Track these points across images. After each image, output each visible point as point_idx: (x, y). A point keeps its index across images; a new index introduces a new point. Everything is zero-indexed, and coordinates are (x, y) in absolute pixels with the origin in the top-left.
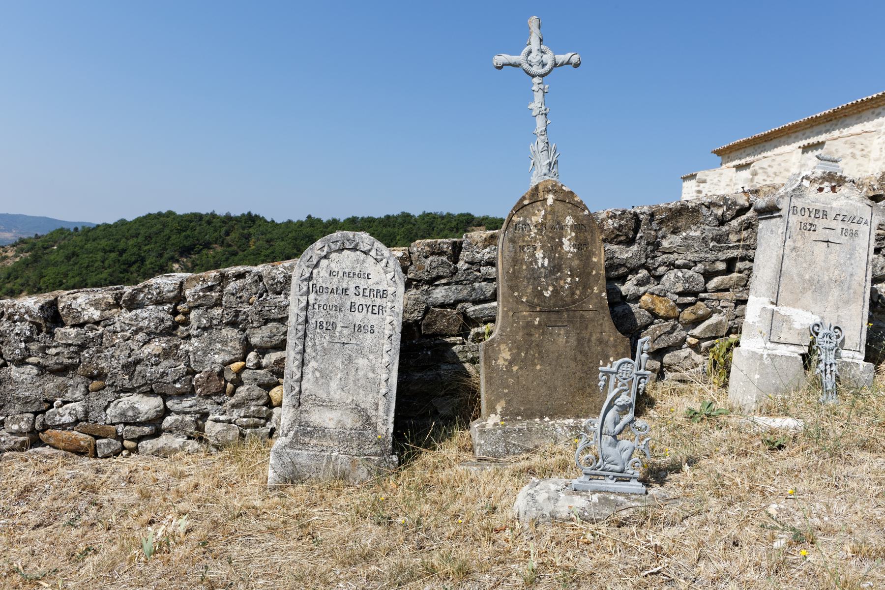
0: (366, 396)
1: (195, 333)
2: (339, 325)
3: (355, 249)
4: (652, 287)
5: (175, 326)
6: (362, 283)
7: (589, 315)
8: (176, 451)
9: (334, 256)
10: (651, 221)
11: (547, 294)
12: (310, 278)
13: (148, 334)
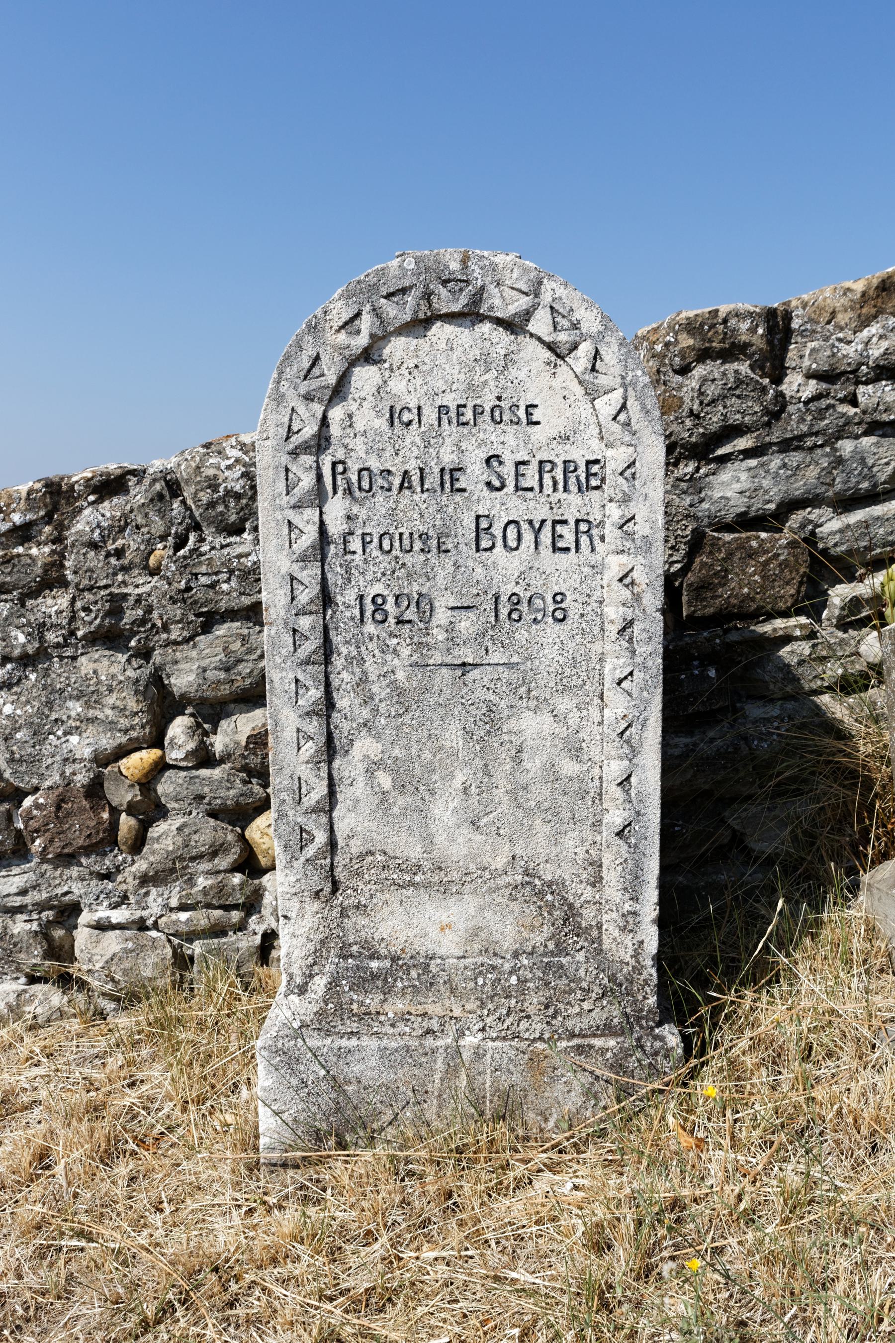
0: (555, 839)
2: (443, 602)
3: (471, 315)
6: (510, 444)
9: (397, 348)
12: (321, 441)
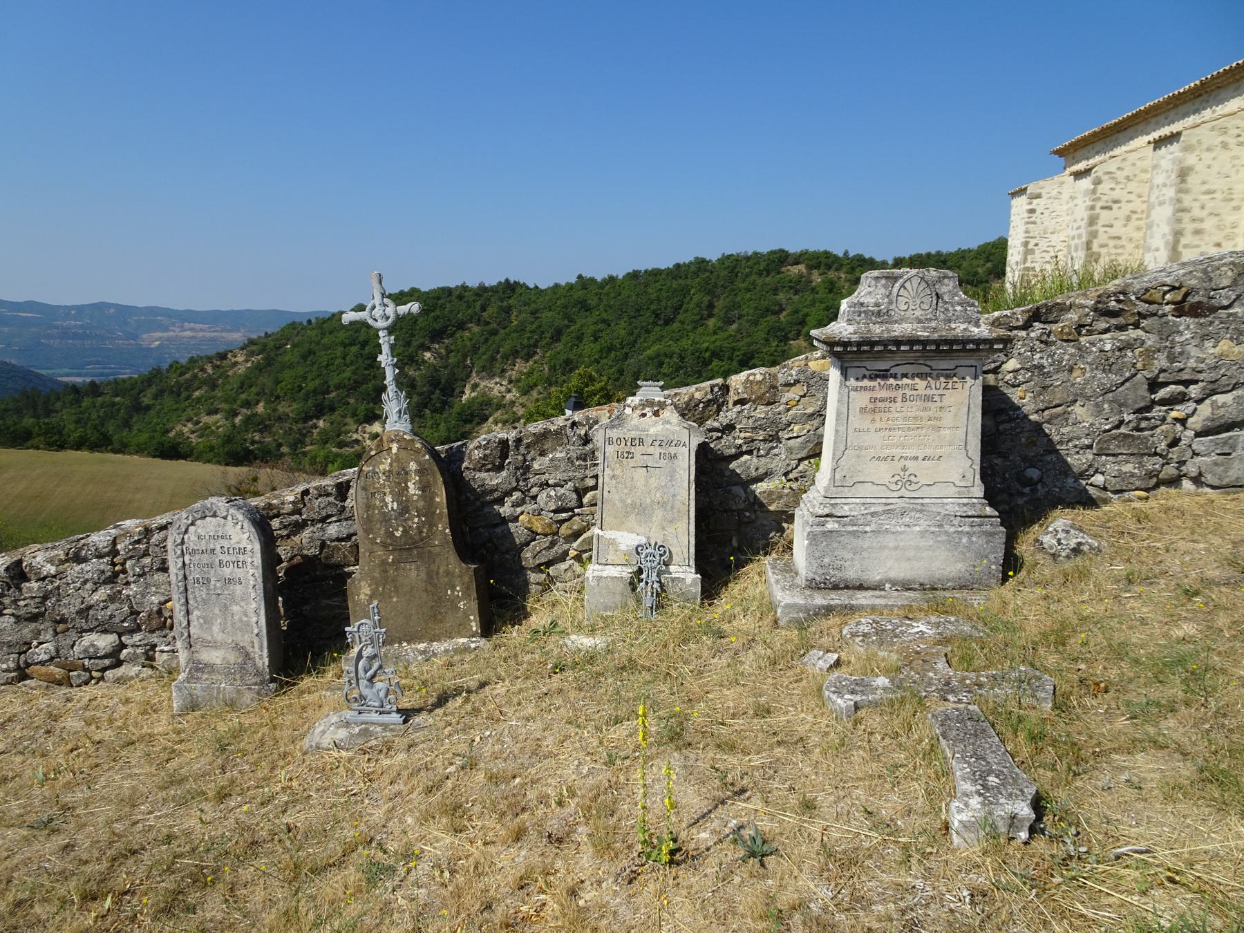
0: (243, 636)
1: (132, 579)
2: (213, 579)
3: (215, 515)
4: (529, 507)
5: (115, 575)
6: (226, 543)
7: (436, 550)
8: (132, 678)
9: (199, 522)
10: (517, 447)
11: (398, 534)
12: (183, 543)
13: (95, 584)
